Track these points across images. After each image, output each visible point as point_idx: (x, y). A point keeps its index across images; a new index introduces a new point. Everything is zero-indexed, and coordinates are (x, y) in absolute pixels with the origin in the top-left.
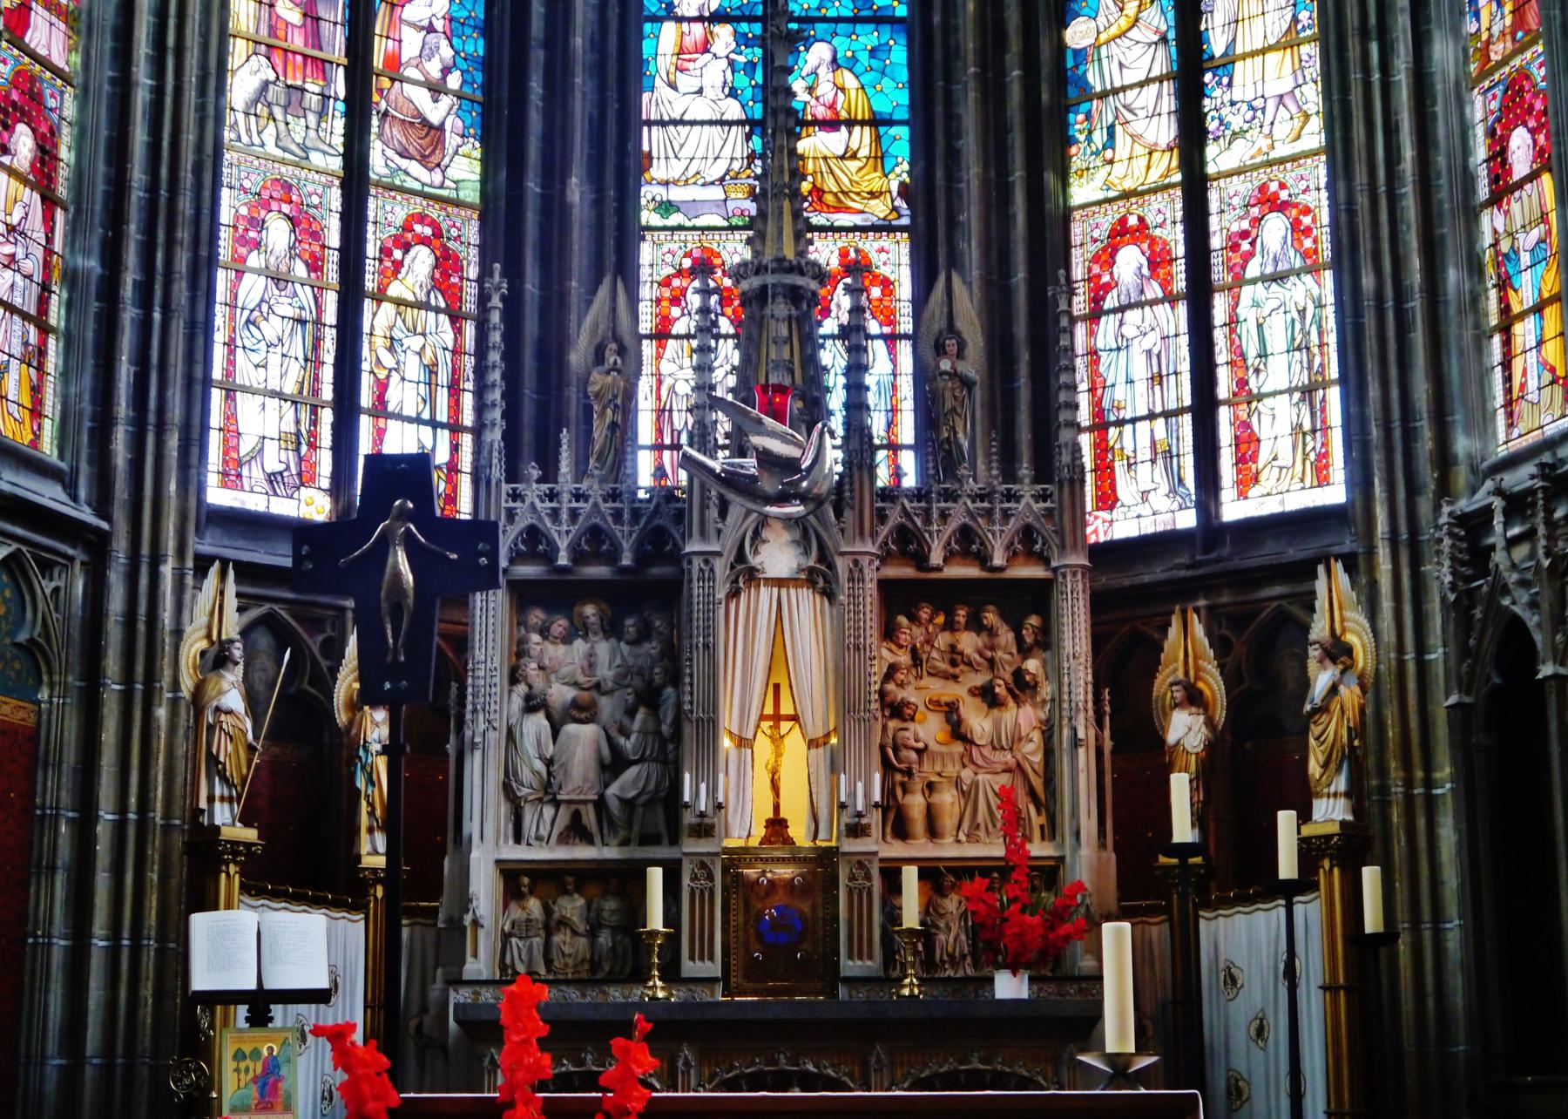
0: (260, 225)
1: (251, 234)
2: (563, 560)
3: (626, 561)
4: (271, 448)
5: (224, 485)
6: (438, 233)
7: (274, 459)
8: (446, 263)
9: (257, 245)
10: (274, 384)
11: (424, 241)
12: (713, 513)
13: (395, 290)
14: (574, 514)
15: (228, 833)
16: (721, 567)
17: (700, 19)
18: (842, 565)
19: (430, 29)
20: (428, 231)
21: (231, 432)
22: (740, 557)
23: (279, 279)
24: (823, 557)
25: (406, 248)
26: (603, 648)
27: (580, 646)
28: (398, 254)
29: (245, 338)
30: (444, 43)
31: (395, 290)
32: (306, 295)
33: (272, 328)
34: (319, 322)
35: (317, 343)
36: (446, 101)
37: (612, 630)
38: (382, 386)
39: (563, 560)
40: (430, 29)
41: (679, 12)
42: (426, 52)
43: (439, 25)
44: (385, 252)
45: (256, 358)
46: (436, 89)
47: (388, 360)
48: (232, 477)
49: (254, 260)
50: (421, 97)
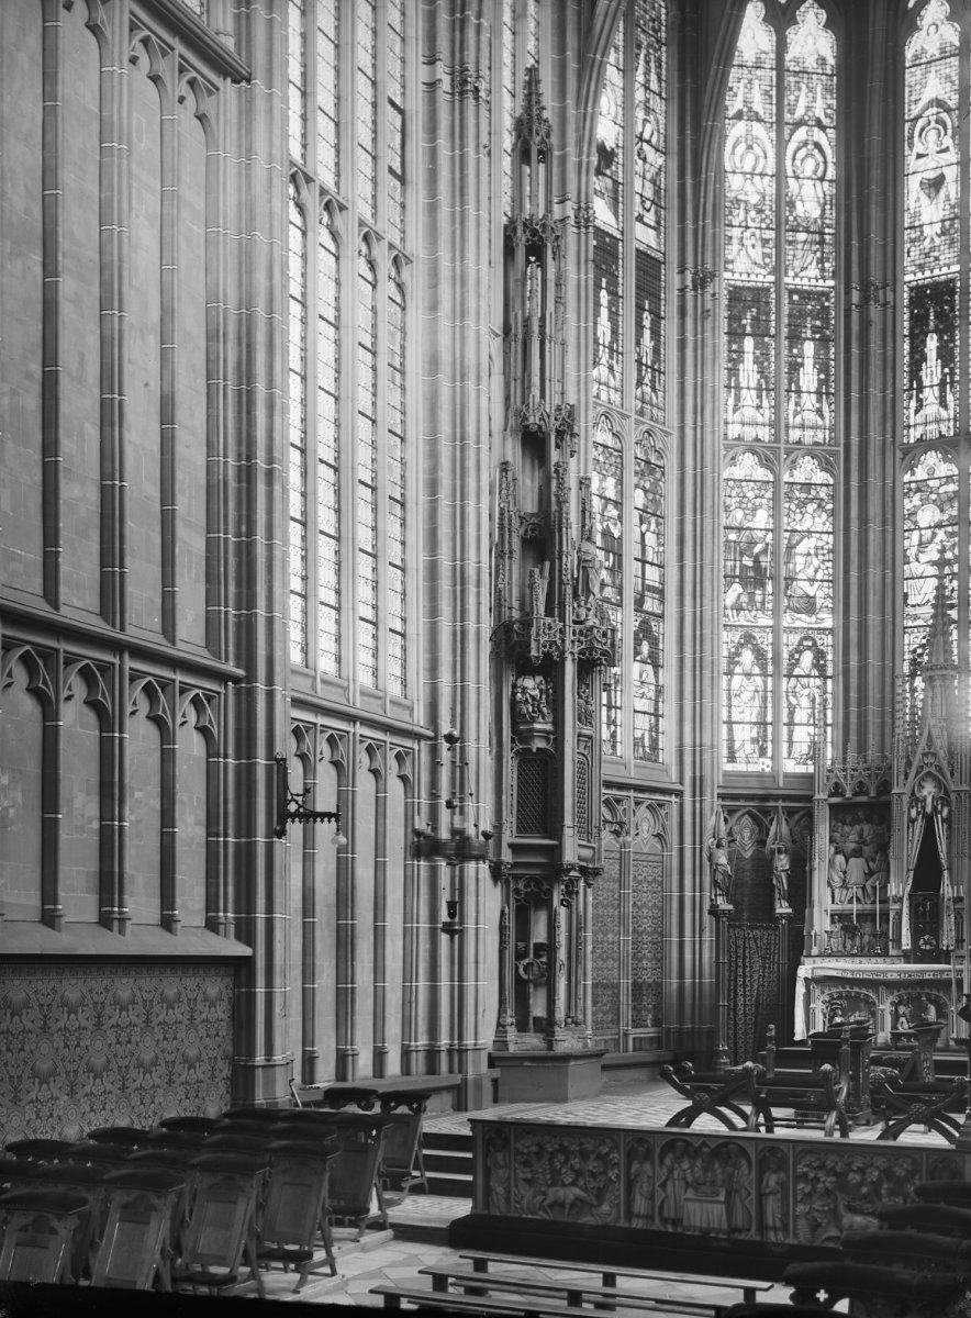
0: (738, 654)
1: (733, 659)
2: (848, 795)
3: (872, 795)
4: (748, 744)
5: (729, 762)
6: (815, 644)
7: (749, 748)
8: (819, 655)
9: (738, 663)
10: (747, 720)
11: (809, 648)
12: (902, 777)
13: (797, 671)
14: (852, 777)
15: (722, 907)
16: (906, 799)
17: (930, 527)
18: (953, 796)
19: (809, 554)
20: (810, 643)
21: (731, 740)
22: (913, 794)
23: (748, 675)
24: (946, 792)
25: (800, 652)
26: (866, 827)
27: (857, 827)
28: (797, 656)
29: (735, 701)
30: (815, 559)
31: (797, 671)
32: (759, 680)
33: (746, 696)
34: (765, 691)
35: (765, 699)
36: (816, 584)
37: (869, 821)
38: (791, 714)
39: (848, 795)
40: (809, 554)
41: (922, 526)
42: (807, 565)
43: (812, 552)
44: (791, 656)
45: (740, 709)
46: (812, 580)
47: (792, 699)
48: (732, 758)
49: (738, 669)
50: (806, 586)
